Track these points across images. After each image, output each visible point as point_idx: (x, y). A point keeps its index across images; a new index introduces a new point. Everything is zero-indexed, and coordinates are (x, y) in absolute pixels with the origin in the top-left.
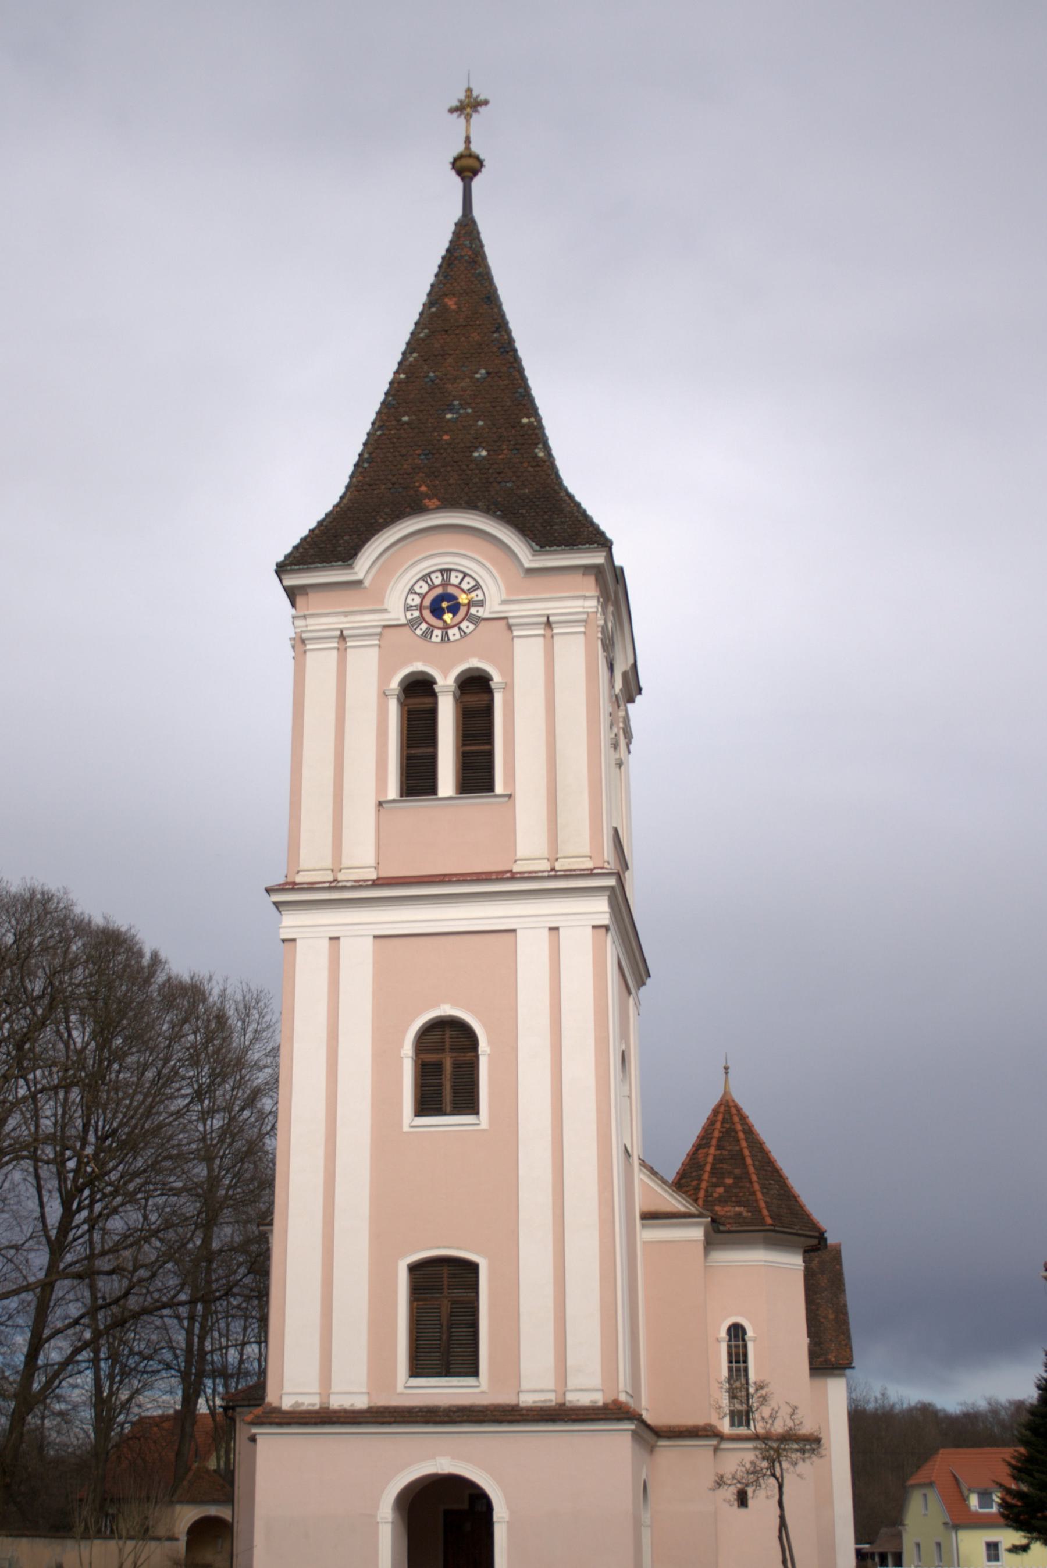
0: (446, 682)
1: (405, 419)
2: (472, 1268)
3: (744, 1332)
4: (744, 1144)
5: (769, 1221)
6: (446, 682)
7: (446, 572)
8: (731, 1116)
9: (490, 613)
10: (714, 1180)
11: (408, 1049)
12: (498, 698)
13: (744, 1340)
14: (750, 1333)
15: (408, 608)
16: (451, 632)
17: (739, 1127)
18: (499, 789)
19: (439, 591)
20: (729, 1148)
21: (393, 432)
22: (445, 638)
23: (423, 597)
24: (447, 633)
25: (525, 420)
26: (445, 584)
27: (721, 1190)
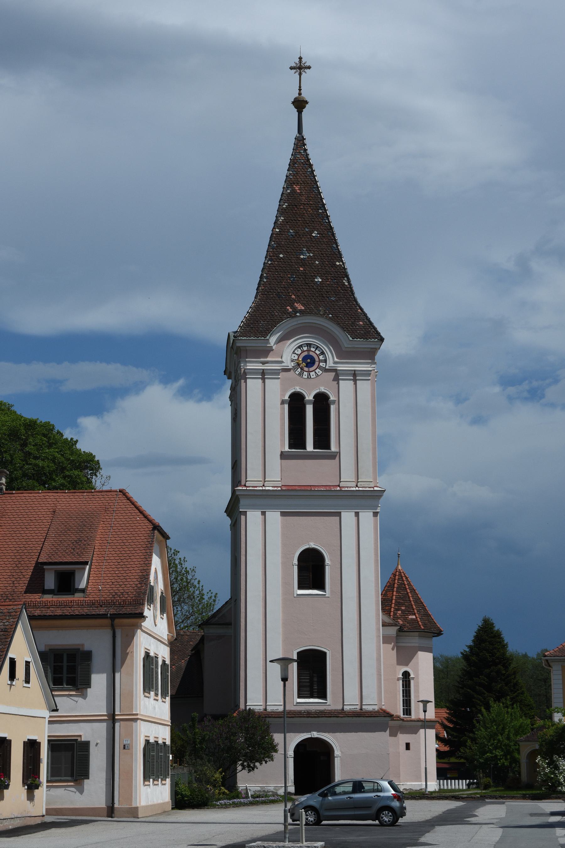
0: (310, 397)
1: (281, 256)
2: (324, 654)
3: (409, 675)
4: (409, 591)
5: (423, 628)
6: (310, 397)
7: (309, 345)
8: (402, 577)
9: (329, 367)
10: (397, 607)
11: (296, 561)
12: (333, 408)
13: (409, 678)
14: (412, 676)
15: (292, 361)
16: (311, 374)
17: (406, 583)
18: (334, 448)
19: (306, 353)
20: (402, 592)
21: (276, 263)
22: (309, 377)
23: (299, 355)
24: (310, 374)
25: (338, 263)
26: (308, 351)
27: (400, 612)
